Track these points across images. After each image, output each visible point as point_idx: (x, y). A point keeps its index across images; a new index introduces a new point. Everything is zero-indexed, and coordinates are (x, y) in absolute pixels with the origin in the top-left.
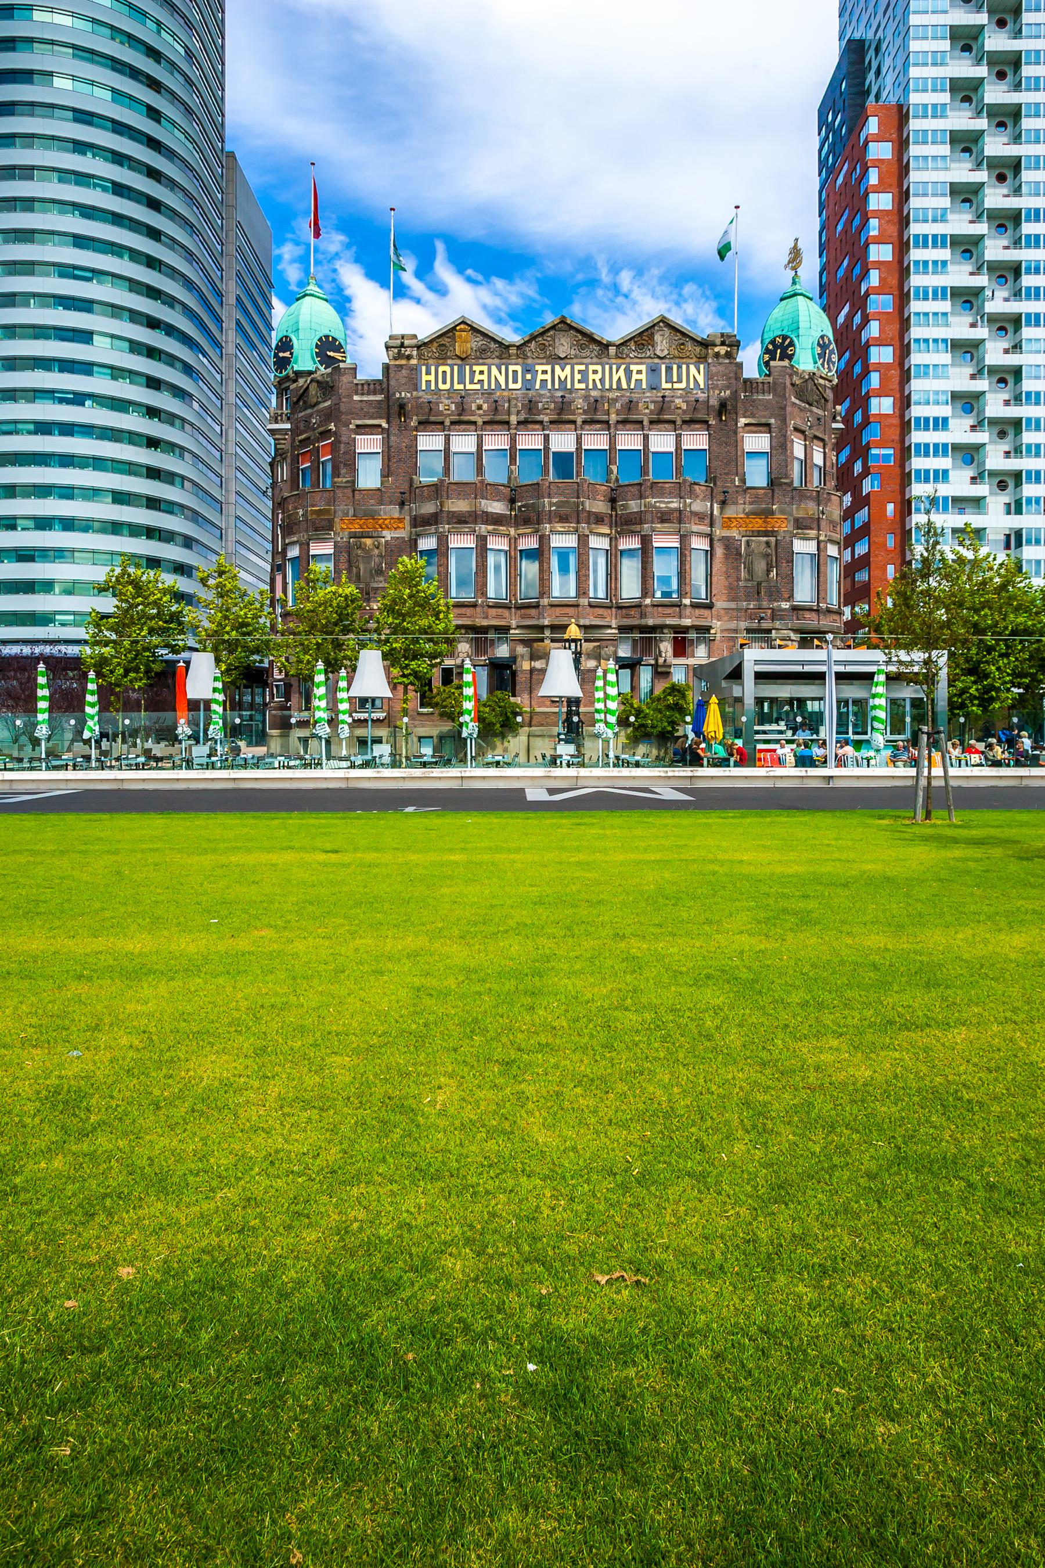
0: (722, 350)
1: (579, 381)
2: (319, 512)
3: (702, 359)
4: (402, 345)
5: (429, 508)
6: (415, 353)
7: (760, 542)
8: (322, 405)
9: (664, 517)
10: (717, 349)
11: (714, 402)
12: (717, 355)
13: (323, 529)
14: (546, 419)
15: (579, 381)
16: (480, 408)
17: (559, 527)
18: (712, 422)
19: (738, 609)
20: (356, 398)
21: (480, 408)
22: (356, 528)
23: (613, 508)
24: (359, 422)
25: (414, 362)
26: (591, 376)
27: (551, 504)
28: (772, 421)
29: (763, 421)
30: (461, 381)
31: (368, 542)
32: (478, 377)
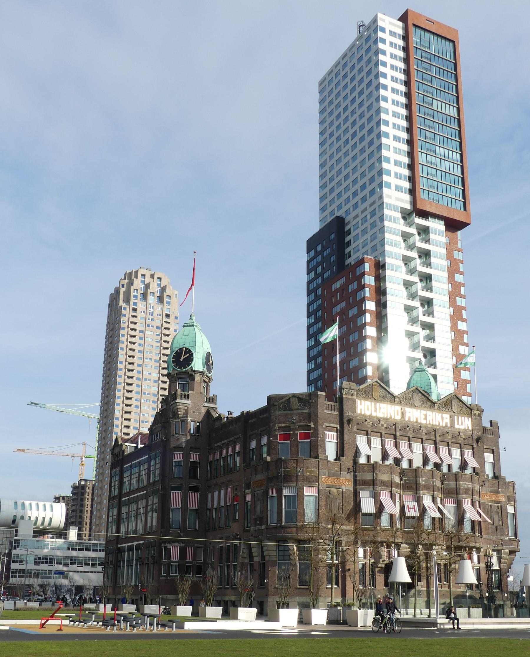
0: (477, 412)
1: (424, 419)
2: (311, 472)
3: (470, 415)
4: (350, 389)
5: (368, 476)
6: (355, 393)
7: (495, 506)
8: (300, 411)
9: (466, 492)
10: (475, 412)
11: (475, 437)
12: (475, 414)
13: (313, 481)
14: (411, 436)
15: (424, 419)
16: (383, 425)
17: (426, 492)
18: (475, 446)
19: (489, 539)
20: (325, 411)
21: (383, 425)
22: (329, 483)
23: (442, 484)
24: (328, 425)
25: (354, 397)
26: (428, 417)
27: (423, 481)
28: (494, 448)
29: (491, 448)
30: (375, 411)
31: (334, 490)
32: (382, 410)
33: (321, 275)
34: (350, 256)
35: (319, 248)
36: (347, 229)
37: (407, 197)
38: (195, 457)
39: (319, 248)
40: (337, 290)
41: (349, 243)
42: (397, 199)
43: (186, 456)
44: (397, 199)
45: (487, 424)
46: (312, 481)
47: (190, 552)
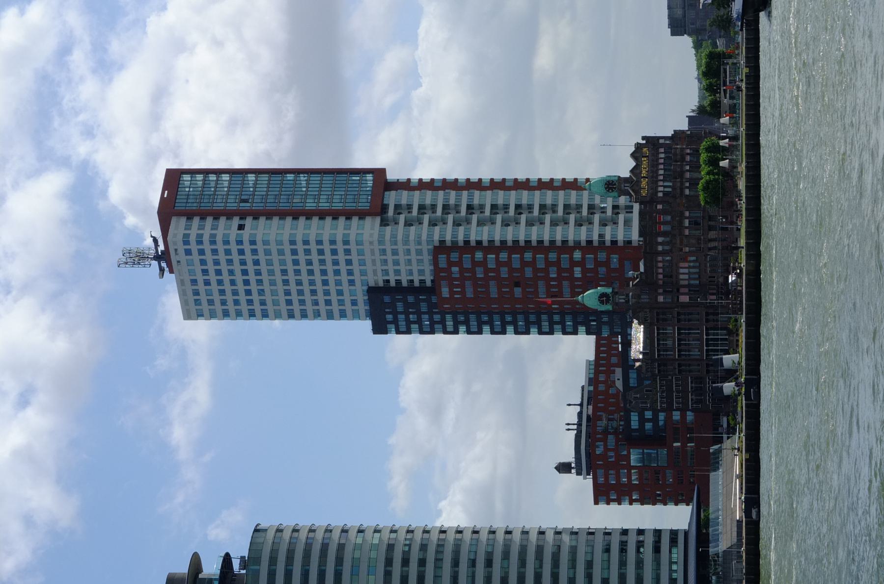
5: (678, 191)
33: (419, 313)
34: (412, 281)
35: (389, 317)
36: (381, 284)
37: (368, 219)
38: (661, 291)
39: (389, 317)
40: (452, 292)
41: (398, 282)
42: (372, 229)
43: (660, 294)
44: (372, 229)
45: (644, 142)
46: (682, 214)
47: (711, 291)
